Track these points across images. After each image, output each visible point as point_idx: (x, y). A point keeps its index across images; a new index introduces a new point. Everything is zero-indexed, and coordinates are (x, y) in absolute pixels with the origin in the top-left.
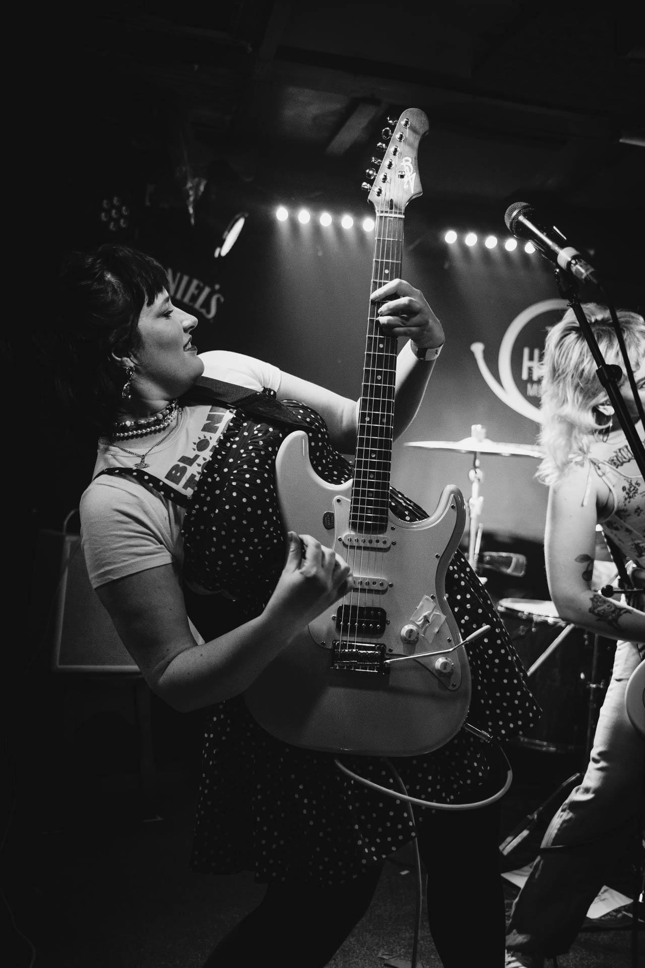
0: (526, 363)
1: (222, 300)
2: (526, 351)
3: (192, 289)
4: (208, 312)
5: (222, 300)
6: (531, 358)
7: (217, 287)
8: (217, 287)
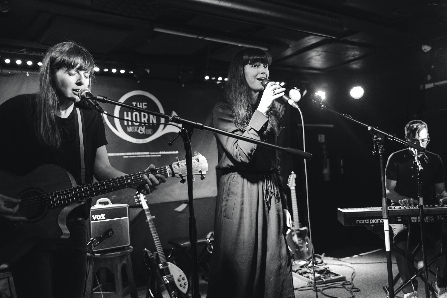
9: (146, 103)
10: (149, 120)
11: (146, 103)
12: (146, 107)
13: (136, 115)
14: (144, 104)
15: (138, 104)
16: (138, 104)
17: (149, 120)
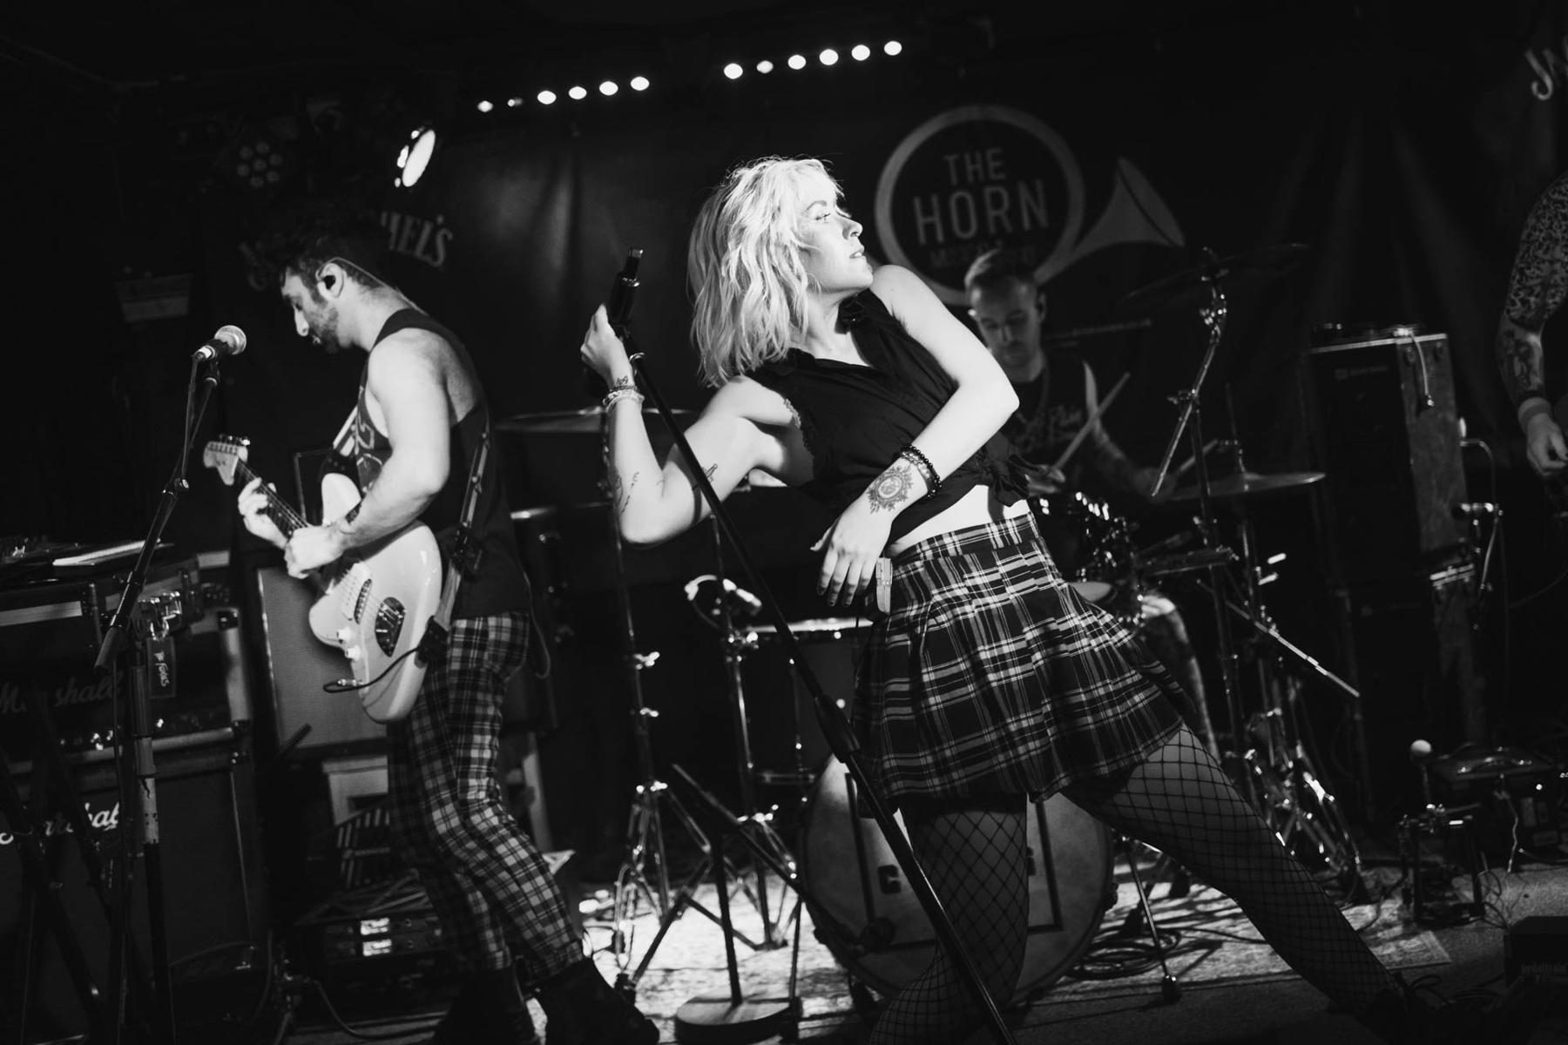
0: (921, 221)
1: (450, 236)
2: (917, 203)
3: (407, 232)
4: (435, 257)
5: (450, 236)
6: (927, 211)
7: (440, 220)
8: (440, 220)
9: (997, 150)
10: (1014, 214)
11: (997, 150)
12: (998, 164)
13: (962, 203)
14: (990, 153)
15: (967, 157)
16: (967, 157)
17: (1014, 214)
